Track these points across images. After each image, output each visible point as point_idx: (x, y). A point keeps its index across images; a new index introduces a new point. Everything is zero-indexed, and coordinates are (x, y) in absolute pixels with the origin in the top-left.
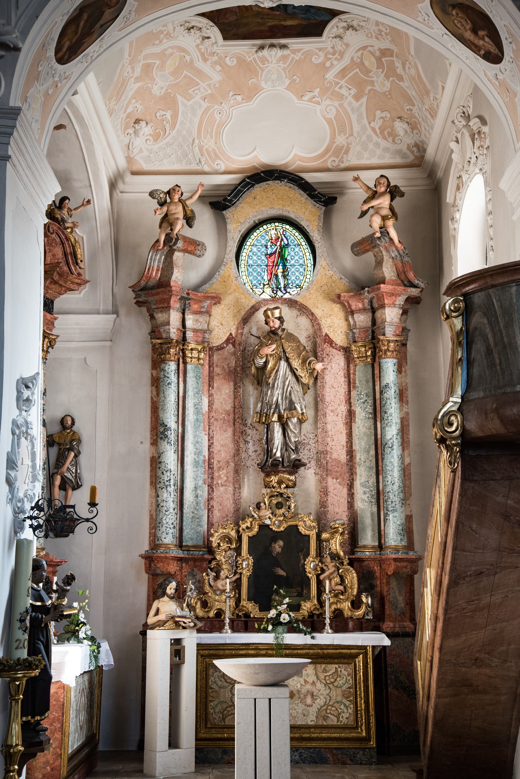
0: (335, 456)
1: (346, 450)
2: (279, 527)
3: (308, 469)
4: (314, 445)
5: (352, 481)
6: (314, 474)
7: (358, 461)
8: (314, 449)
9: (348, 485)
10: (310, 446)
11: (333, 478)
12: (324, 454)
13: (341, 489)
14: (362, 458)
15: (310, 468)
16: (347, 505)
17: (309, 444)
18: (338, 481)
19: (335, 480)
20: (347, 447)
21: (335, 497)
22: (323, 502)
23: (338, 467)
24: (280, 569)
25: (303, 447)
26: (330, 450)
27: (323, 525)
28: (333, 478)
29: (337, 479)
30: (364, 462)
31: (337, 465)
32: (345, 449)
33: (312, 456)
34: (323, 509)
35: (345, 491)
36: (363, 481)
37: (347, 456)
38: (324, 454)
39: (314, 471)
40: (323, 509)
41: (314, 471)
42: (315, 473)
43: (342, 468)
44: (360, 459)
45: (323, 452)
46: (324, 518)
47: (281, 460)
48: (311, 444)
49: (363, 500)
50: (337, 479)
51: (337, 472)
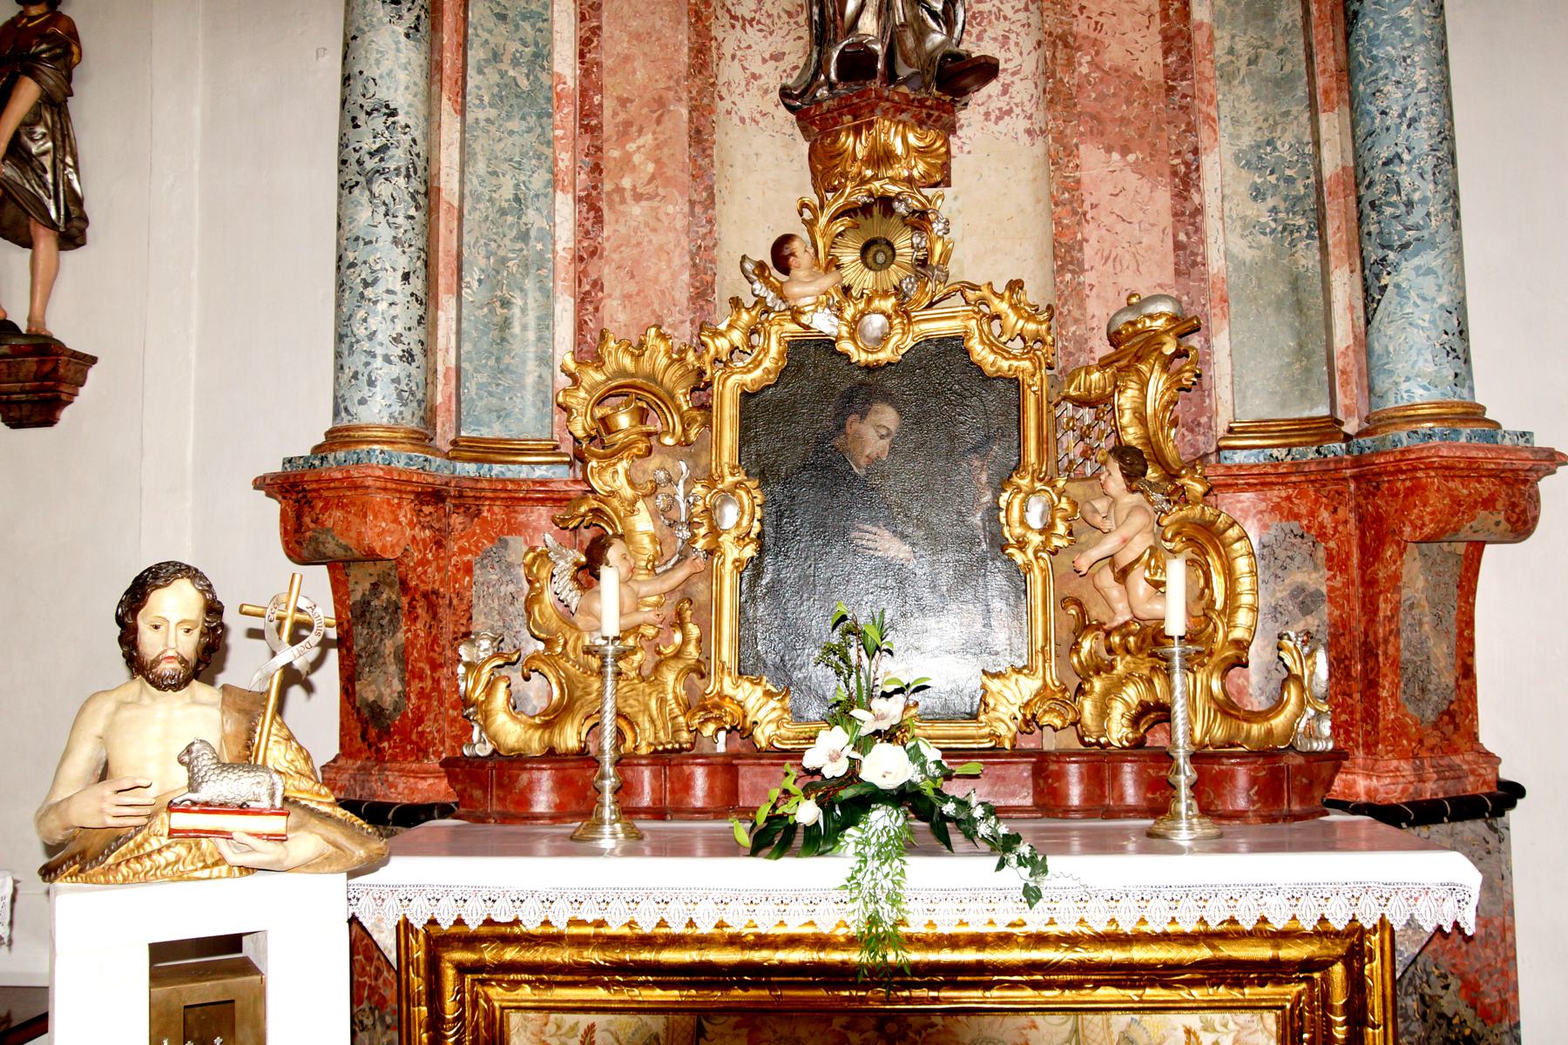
0: (1114, 55)
1: (1163, 32)
2: (883, 340)
3: (999, 118)
4: (1022, 16)
5: (1190, 157)
6: (1025, 138)
7: (1224, 59)
8: (1023, 31)
9: (1175, 173)
10: (1006, 25)
11: (1109, 150)
12: (1066, 45)
13: (1146, 191)
14: (1240, 46)
15: (1009, 112)
16: (1171, 258)
17: (999, 15)
18: (1131, 158)
19: (1116, 156)
20: (1165, 17)
21: (1120, 227)
22: (1070, 248)
23: (1129, 102)
24: (887, 534)
25: (975, 31)
26: (1093, 35)
27: (1071, 346)
28: (1109, 150)
29: (1125, 151)
30: (1252, 62)
31: (1123, 94)
32: (1157, 24)
33: (1017, 61)
34: (1068, 277)
35: (1163, 198)
36: (1246, 141)
37: (1166, 53)
38: (1066, 45)
39: (1026, 124)
40: (1068, 277)
41: (1026, 124)
42: (1029, 132)
43: (1146, 105)
44: (1231, 51)
45: (1063, 38)
46: (1076, 313)
47: (878, 47)
48: (1009, 13)
49: (1250, 227)
50: (1125, 151)
51: (1124, 121)
